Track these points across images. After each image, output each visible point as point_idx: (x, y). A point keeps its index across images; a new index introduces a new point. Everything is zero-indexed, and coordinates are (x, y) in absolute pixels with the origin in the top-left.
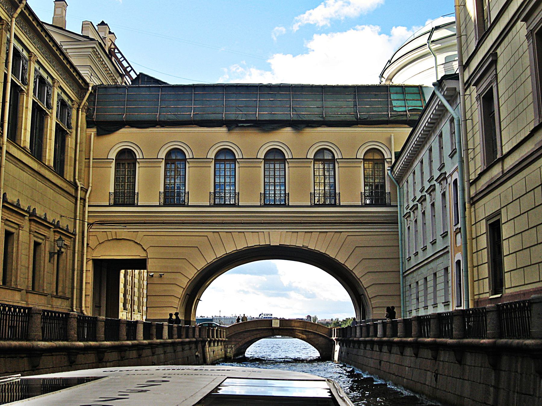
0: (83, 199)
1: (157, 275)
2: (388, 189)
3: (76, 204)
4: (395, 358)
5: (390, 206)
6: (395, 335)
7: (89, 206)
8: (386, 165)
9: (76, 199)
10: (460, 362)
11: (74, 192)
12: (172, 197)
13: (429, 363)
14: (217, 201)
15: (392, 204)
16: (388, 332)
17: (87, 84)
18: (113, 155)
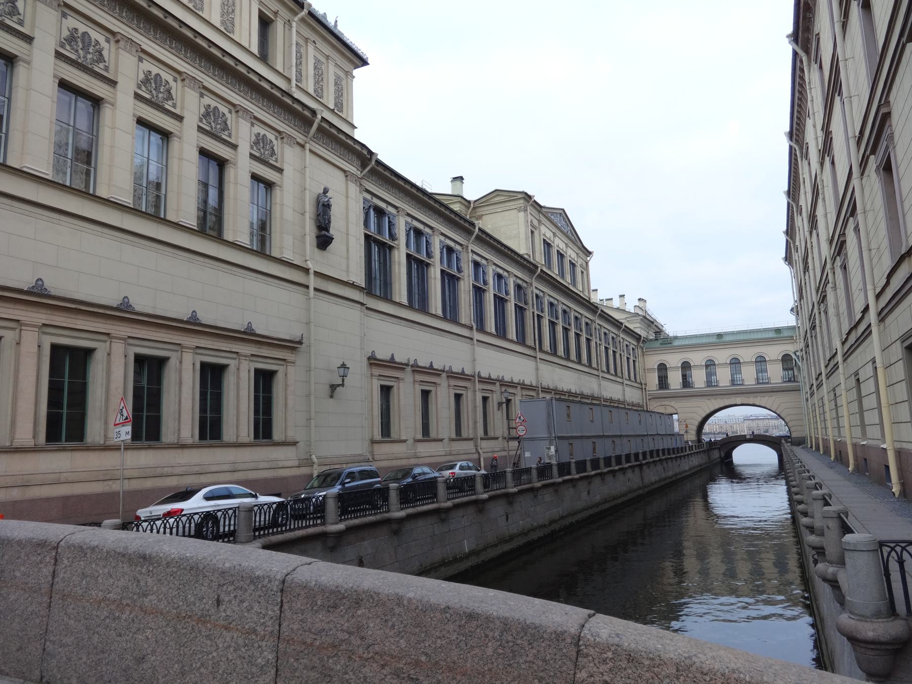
11: (642, 387)
12: (686, 383)
18: (656, 367)
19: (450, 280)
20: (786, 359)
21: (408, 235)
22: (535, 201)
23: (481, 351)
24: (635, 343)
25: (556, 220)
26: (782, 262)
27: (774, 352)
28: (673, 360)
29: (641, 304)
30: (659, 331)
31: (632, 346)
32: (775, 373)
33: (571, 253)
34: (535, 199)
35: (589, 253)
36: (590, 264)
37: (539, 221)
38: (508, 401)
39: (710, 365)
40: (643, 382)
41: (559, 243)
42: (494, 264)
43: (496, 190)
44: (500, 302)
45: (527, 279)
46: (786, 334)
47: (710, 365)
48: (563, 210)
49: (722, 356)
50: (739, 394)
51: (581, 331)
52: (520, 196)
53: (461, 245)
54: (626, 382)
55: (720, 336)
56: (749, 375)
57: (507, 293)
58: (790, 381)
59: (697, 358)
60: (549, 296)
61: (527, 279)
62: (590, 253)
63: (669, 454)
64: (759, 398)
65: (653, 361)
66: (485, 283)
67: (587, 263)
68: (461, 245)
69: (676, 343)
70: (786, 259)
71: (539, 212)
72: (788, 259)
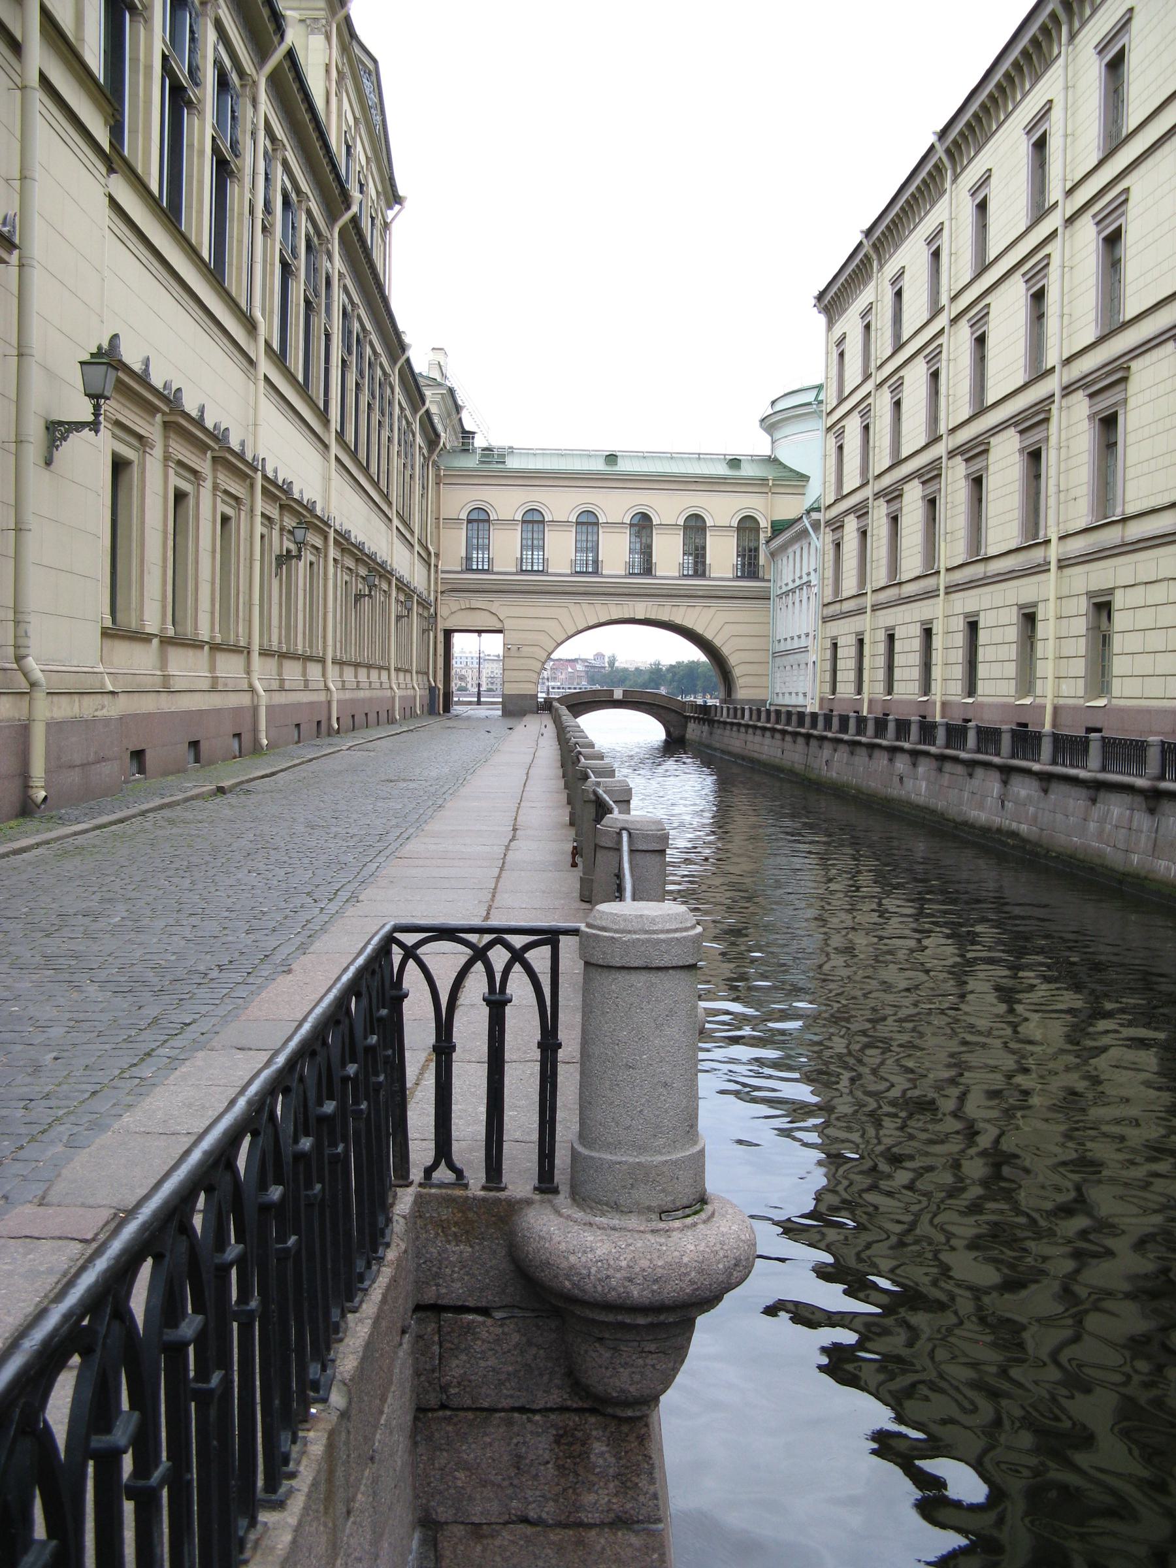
0: (436, 566)
1: (514, 648)
2: (762, 560)
3: (429, 570)
4: (758, 739)
5: (763, 580)
6: (777, 722)
7: (443, 572)
8: (762, 536)
9: (430, 565)
10: (808, 744)
13: (779, 743)
14: (578, 569)
15: (766, 577)
16: (754, 717)
17: (438, 436)
20: (747, 526)
22: (348, 20)
25: (367, 85)
26: (813, 301)
27: (722, 510)
28: (507, 503)
29: (439, 357)
32: (722, 555)
35: (393, 197)
36: (395, 227)
39: (588, 523)
46: (748, 470)
47: (588, 523)
49: (616, 507)
50: (637, 596)
55: (611, 458)
56: (669, 554)
57: (295, 255)
58: (742, 577)
59: (562, 505)
63: (788, 723)
64: (682, 609)
65: (459, 501)
67: (386, 225)
69: (513, 463)
70: (821, 296)
72: (832, 301)
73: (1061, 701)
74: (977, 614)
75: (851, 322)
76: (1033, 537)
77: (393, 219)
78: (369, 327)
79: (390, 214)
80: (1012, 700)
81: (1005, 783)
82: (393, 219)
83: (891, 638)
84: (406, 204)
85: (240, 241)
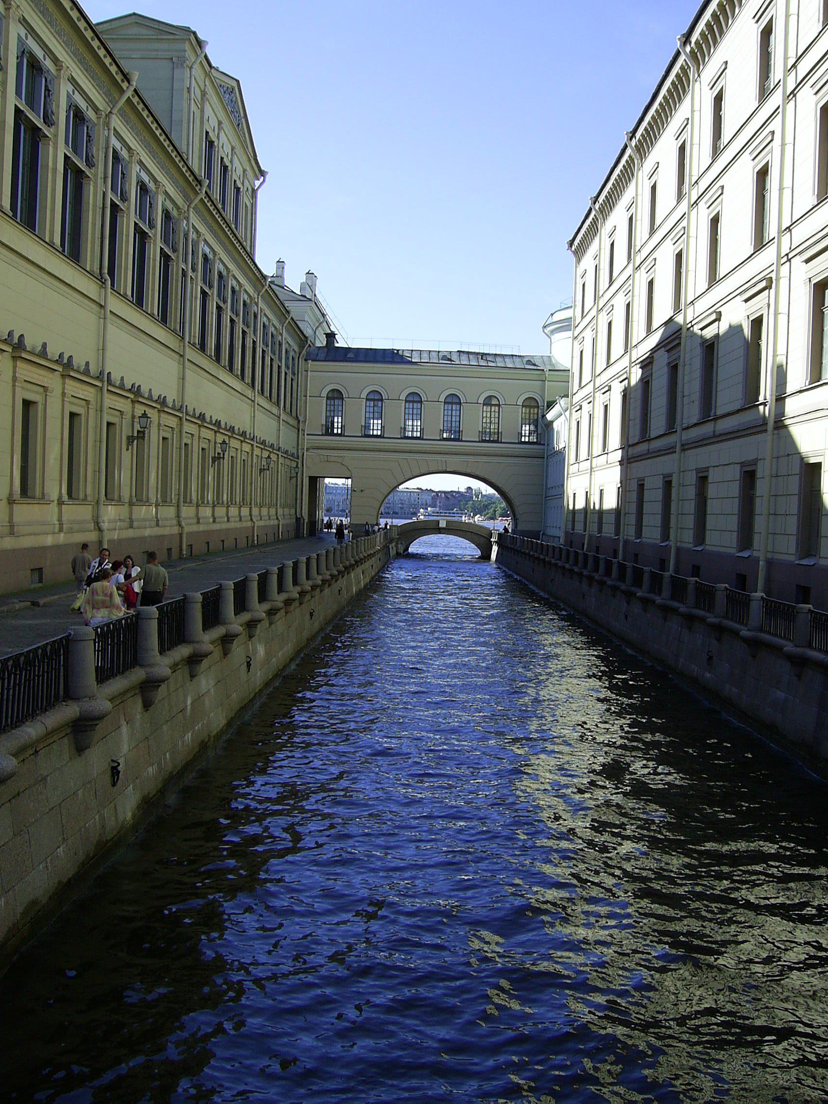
0: (303, 430)
18: (324, 394)
19: (76, 178)
21: (19, 66)
23: (116, 334)
24: (296, 349)
30: (331, 336)
31: (292, 354)
33: (237, 168)
34: (209, 50)
36: (260, 193)
37: (204, 94)
38: (141, 435)
40: (301, 419)
41: (225, 143)
42: (144, 165)
43: (134, 14)
44: (142, 237)
45: (180, 201)
48: (238, 81)
51: (237, 315)
52: (181, 35)
53: (96, 110)
54: (283, 416)
60: (209, 242)
61: (180, 201)
62: (263, 173)
66: (124, 198)
67: (254, 192)
68: (96, 110)
71: (207, 75)
73: (684, 545)
74: (707, 469)
75: (588, 262)
76: (671, 428)
77: (259, 187)
78: (231, 266)
79: (257, 183)
80: (658, 542)
81: (628, 603)
82: (259, 187)
83: (641, 487)
84: (267, 177)
85: (94, 224)
